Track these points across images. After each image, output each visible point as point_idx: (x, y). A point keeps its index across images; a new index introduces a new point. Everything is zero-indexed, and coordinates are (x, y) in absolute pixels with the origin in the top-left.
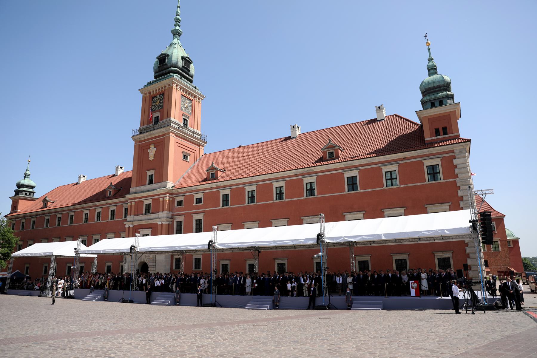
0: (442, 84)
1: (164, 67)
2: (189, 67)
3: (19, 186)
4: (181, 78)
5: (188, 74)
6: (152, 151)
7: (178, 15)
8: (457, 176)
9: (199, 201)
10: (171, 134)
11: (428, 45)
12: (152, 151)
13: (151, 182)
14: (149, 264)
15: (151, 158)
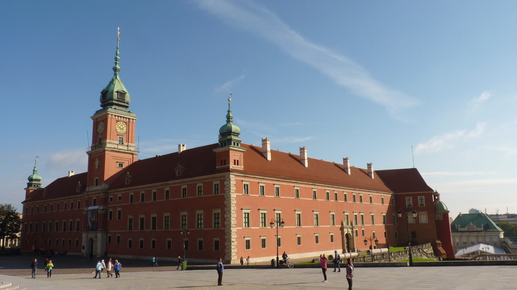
0: (226, 131)
1: (107, 99)
2: (124, 97)
3: (31, 179)
4: (115, 109)
5: (124, 102)
6: (97, 163)
7: (117, 55)
8: (224, 192)
9: (120, 198)
10: (106, 152)
11: (229, 101)
12: (97, 163)
13: (97, 185)
14: (94, 240)
15: (96, 168)
